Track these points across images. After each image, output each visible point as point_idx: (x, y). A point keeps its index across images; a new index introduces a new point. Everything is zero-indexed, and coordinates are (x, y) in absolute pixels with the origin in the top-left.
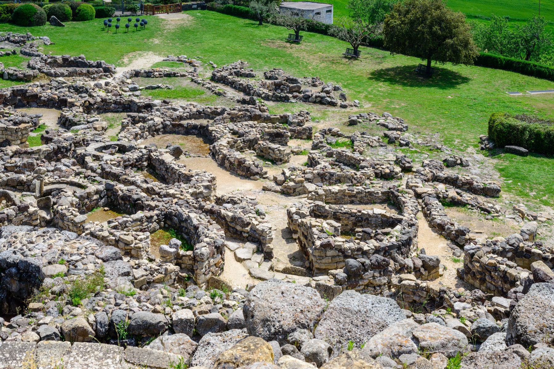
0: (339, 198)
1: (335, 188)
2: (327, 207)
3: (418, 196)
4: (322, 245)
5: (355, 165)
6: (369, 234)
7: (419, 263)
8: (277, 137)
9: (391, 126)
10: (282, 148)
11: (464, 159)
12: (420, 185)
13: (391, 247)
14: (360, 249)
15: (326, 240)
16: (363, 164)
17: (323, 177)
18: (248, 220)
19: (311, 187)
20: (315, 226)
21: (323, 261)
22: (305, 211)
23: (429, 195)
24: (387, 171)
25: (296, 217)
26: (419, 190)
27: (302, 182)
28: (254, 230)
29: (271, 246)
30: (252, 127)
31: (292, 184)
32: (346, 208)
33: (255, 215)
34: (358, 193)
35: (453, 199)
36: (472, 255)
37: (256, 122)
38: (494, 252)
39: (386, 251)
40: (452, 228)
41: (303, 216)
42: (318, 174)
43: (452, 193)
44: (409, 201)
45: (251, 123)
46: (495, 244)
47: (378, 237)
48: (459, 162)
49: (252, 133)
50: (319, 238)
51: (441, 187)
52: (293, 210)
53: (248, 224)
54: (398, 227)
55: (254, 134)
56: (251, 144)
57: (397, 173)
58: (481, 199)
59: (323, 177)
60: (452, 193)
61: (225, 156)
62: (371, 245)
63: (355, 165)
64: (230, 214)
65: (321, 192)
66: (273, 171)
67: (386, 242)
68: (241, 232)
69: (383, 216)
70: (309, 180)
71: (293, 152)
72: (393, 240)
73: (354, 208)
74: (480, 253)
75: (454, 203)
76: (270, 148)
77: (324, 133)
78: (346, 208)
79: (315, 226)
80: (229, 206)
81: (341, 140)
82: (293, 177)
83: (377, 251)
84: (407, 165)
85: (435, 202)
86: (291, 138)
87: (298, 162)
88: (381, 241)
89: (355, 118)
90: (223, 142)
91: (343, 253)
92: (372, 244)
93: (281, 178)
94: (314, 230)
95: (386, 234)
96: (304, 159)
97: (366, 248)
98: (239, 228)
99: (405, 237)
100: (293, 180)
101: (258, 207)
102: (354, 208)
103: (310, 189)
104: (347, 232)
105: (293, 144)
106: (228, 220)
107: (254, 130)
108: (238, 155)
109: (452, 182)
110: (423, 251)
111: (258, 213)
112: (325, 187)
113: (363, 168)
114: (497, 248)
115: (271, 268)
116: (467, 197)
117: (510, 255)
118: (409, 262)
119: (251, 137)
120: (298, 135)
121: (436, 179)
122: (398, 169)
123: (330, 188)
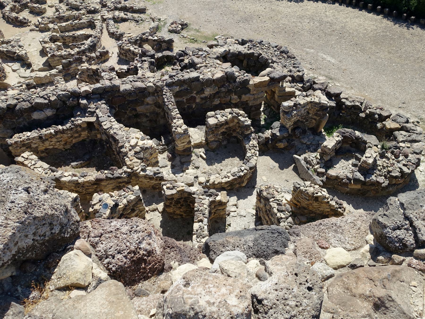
0: (64, 30)
1: (64, 24)
2: (58, 35)
3: (104, 20)
4: (51, 56)
5: (77, 9)
6: (75, 45)
7: (98, 54)
10: (40, 6)
12: (107, 14)
13: (86, 49)
14: (70, 54)
15: (52, 54)
16: (81, 7)
18: (14, 51)
19: (51, 26)
20: (47, 48)
21: (54, 62)
22: (47, 39)
24: (93, 9)
26: (105, 17)
27: (48, 23)
28: (18, 55)
29: (29, 61)
31: (43, 25)
33: (18, 48)
34: (76, 24)
35: (122, 18)
36: (120, 46)
38: (130, 42)
39: (83, 52)
40: (117, 34)
41: (46, 42)
42: (57, 17)
43: (122, 15)
44: (98, 24)
47: (79, 46)
50: (50, 53)
51: (117, 13)
52: (41, 40)
53: (15, 53)
54: (90, 39)
57: (98, 9)
58: (136, 15)
60: (122, 15)
61: (8, 16)
63: (77, 9)
64: (6, 50)
65: (56, 27)
66: (34, 20)
67: (82, 48)
68: (13, 57)
70: (50, 22)
71: (49, 6)
72: (86, 46)
73: (71, 34)
74: (123, 45)
75: (124, 20)
76: (34, 7)
80: (4, 45)
82: (43, 22)
83: (78, 53)
84: (104, 3)
85: (112, 22)
88: (80, 48)
90: (7, 8)
91: (62, 57)
92: (76, 50)
93: (38, 23)
95: (84, 44)
97: (73, 53)
98: (12, 56)
99: (92, 44)
100: (43, 24)
101: (20, 43)
102: (71, 34)
103: (51, 27)
104: (66, 46)
106: (5, 52)
108: (14, 15)
109: (125, 9)
110: (104, 48)
111: (20, 46)
112: (59, 24)
113: (80, 10)
114: (132, 40)
115: (32, 71)
116: (130, 15)
117: (139, 42)
118: (93, 55)
121: (116, 9)
123: (61, 24)
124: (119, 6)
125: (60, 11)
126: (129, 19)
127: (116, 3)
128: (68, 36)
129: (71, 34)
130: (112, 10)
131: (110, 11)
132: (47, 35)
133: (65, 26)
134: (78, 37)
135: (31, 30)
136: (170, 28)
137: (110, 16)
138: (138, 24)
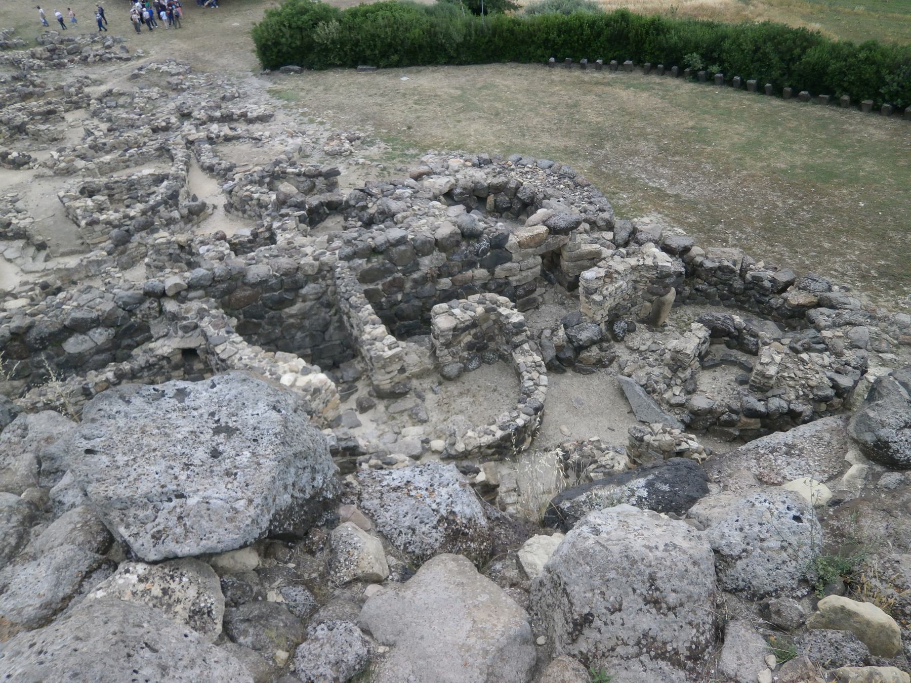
1: (107, 158)
4: (87, 224)
8: (49, 115)
9: (173, 72)
11: (241, 91)
12: (194, 131)
13: (158, 204)
16: (139, 123)
17: (97, 148)
19: (80, 164)
20: (78, 208)
22: (74, 192)
23: (200, 140)
25: (65, 200)
26: (191, 138)
30: (20, 110)
31: (63, 165)
32: (116, 176)
33: (15, 214)
37: (23, 103)
38: (252, 182)
39: (154, 209)
43: (226, 130)
44: (180, 153)
45: (18, 105)
46: (252, 175)
48: (237, 95)
49: (18, 118)
50: (84, 218)
51: (214, 127)
52: (62, 194)
54: (165, 183)
55: (22, 117)
56: (20, 129)
59: (97, 148)
60: (226, 130)
62: (138, 209)
65: (91, 165)
67: (152, 202)
69: (152, 175)
72: (159, 198)
74: (236, 189)
77: (100, 100)
78: (116, 176)
79: (78, 208)
81: (121, 101)
83: (144, 213)
84: (186, 111)
86: (67, 111)
87: (75, 138)
88: (147, 202)
89: (136, 71)
92: (140, 207)
94: (78, 211)
95: (154, 193)
96: (81, 132)
97: (132, 213)
99: (170, 192)
105: (70, 117)
107: (20, 114)
109: (227, 118)
110: (195, 198)
113: (138, 127)
114: (253, 178)
116: (241, 128)
117: (267, 180)
118: (176, 214)
119: (18, 121)
120: (77, 106)
121: (212, 119)
122: (173, 120)
124: (218, 114)
125: (96, 133)
126: (240, 137)
127: (211, 108)
128: (116, 182)
129: (125, 178)
130: (204, 123)
131: (201, 125)
132: (73, 184)
133: (109, 163)
134: (138, 181)
135: (38, 177)
136: (326, 148)
137: (202, 134)
138: (260, 144)
